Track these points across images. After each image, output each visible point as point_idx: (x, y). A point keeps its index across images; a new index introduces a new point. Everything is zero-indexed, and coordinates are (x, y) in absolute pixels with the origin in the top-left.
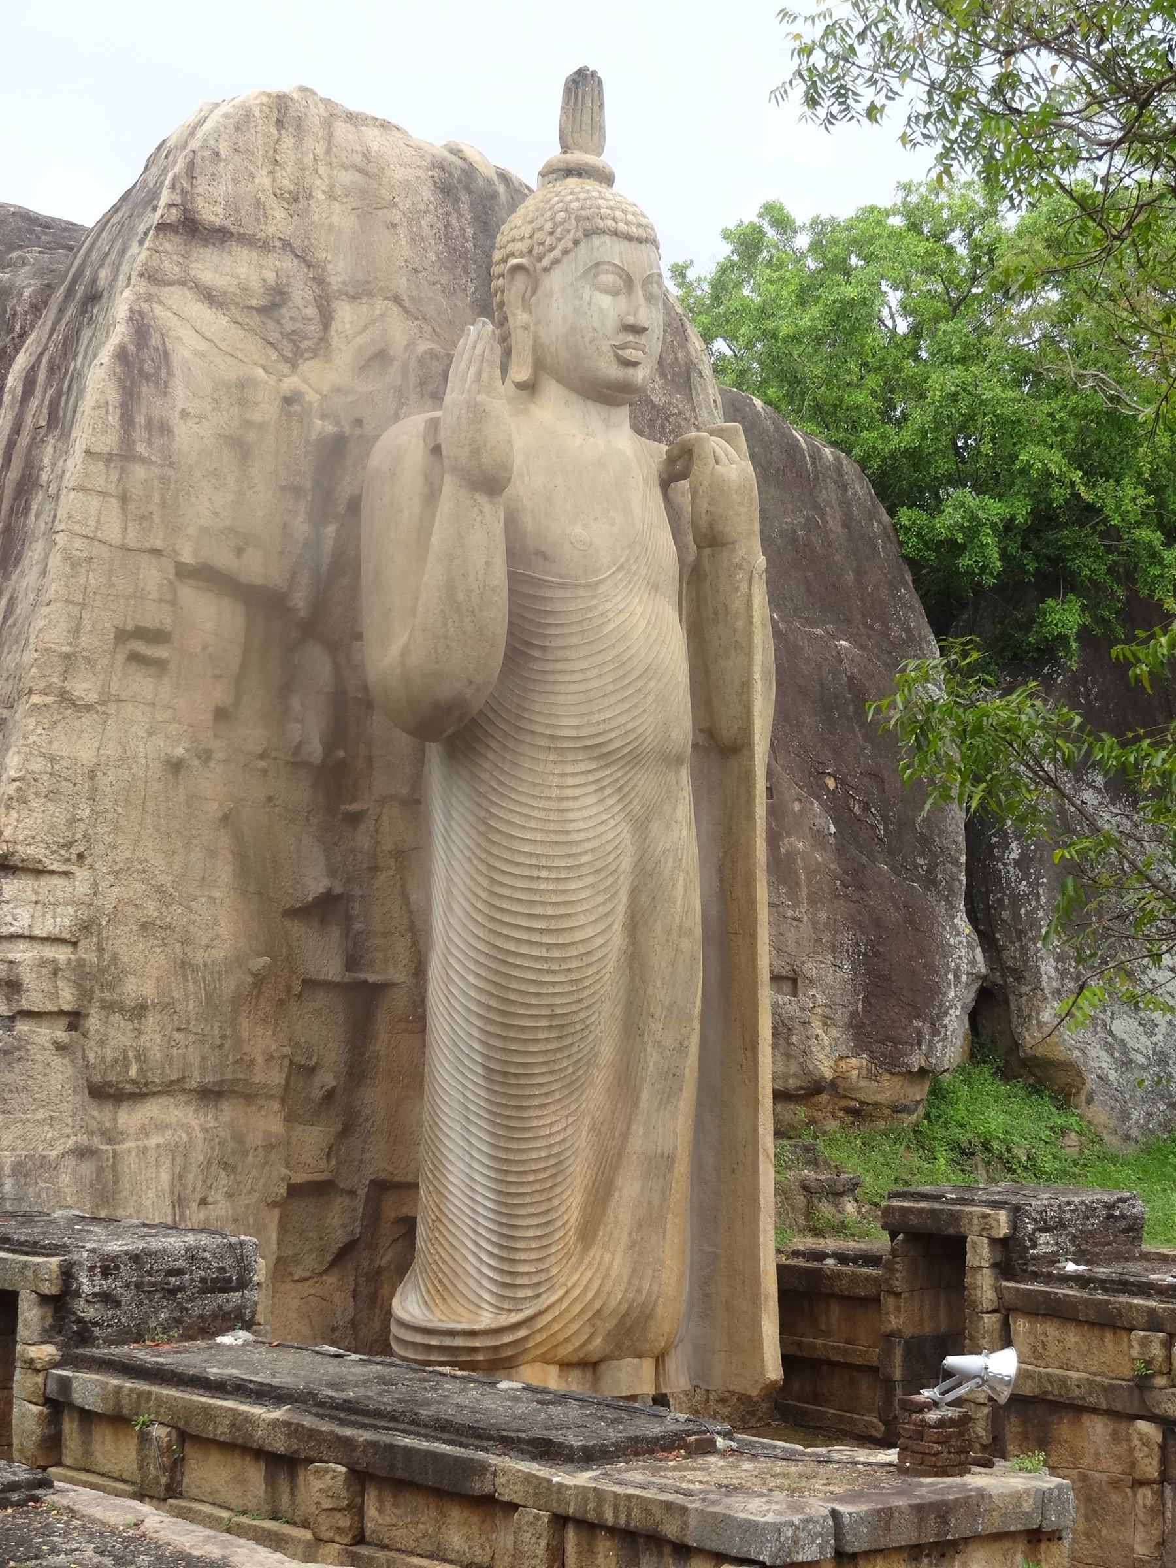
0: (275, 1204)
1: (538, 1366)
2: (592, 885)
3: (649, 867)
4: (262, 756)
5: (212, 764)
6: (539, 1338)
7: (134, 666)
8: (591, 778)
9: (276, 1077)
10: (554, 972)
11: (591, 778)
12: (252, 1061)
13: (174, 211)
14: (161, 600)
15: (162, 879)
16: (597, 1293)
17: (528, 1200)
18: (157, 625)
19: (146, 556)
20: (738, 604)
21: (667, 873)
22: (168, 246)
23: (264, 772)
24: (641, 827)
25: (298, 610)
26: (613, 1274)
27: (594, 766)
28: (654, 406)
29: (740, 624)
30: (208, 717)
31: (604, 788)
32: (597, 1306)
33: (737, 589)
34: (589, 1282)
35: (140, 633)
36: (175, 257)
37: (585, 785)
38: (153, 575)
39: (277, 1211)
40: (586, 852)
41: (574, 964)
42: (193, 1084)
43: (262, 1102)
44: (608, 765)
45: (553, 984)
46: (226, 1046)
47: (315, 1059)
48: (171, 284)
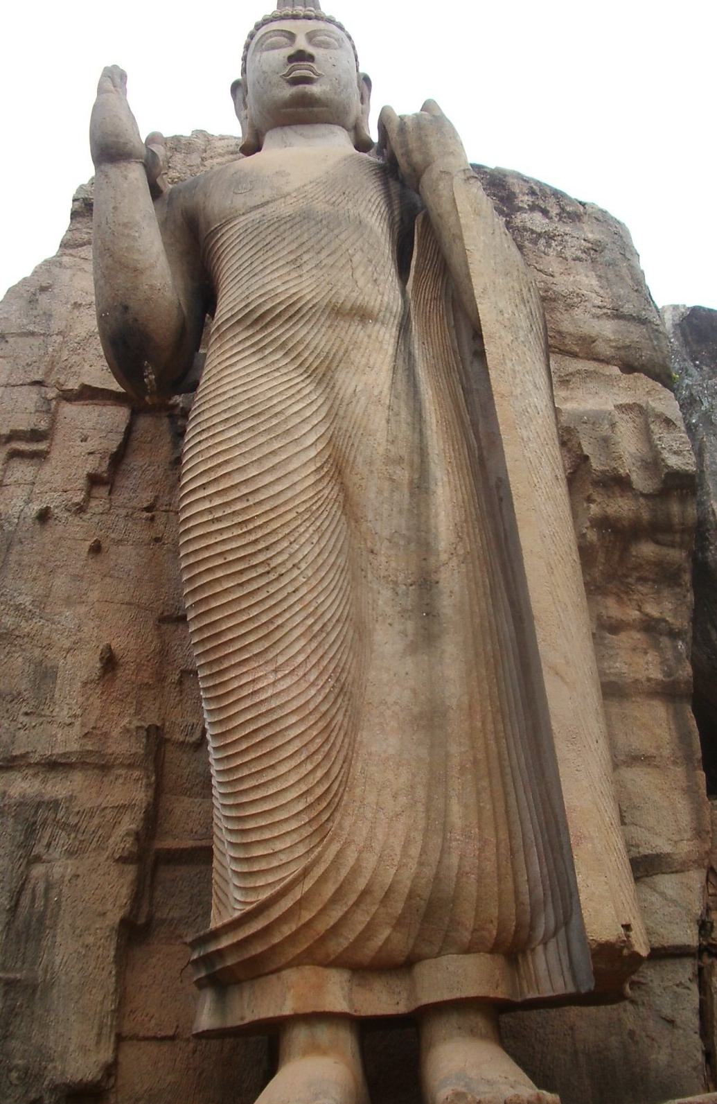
0: (123, 860)
1: (308, 971)
2: (251, 429)
3: (341, 413)
4: (148, 509)
5: (88, 516)
6: (287, 930)
7: (15, 463)
8: (248, 343)
9: (132, 747)
10: (218, 520)
11: (248, 343)
12: (106, 735)
13: (76, 203)
14: (37, 411)
15: (20, 600)
16: (355, 871)
17: (246, 772)
18: (32, 426)
19: (27, 387)
20: (446, 207)
21: (359, 410)
22: (79, 226)
23: (152, 519)
24: (323, 373)
25: (178, 404)
26: (377, 846)
27: (250, 332)
28: (533, 232)
29: (452, 220)
30: (82, 483)
31: (264, 348)
32: (361, 884)
33: (440, 197)
34: (339, 855)
35: (14, 436)
36: (84, 230)
37: (243, 350)
38: (30, 398)
39: (131, 871)
40: (242, 403)
41: (238, 506)
42: (35, 758)
43: (119, 772)
44: (263, 329)
45: (220, 531)
46: (77, 723)
47: (198, 735)
48: (81, 245)
